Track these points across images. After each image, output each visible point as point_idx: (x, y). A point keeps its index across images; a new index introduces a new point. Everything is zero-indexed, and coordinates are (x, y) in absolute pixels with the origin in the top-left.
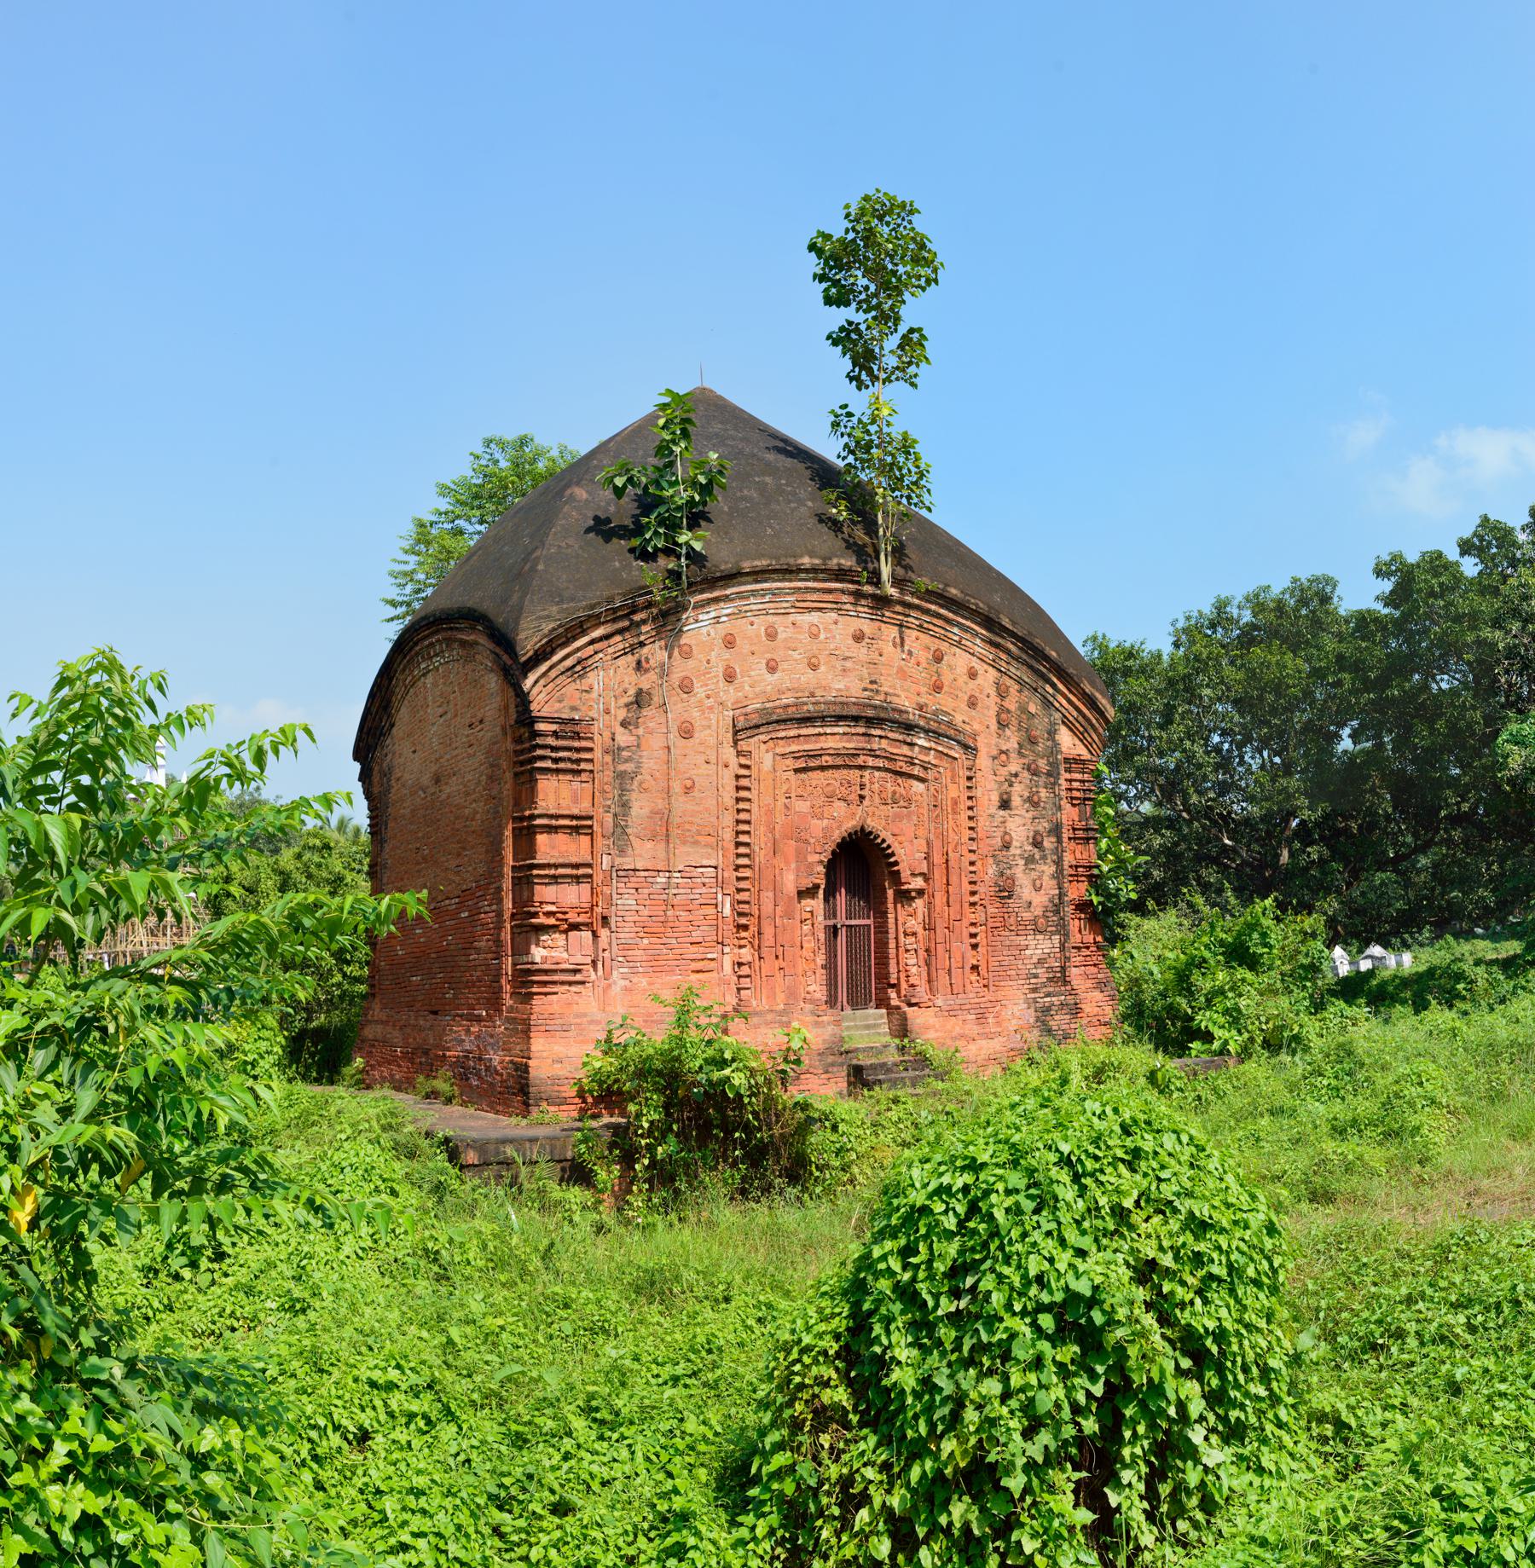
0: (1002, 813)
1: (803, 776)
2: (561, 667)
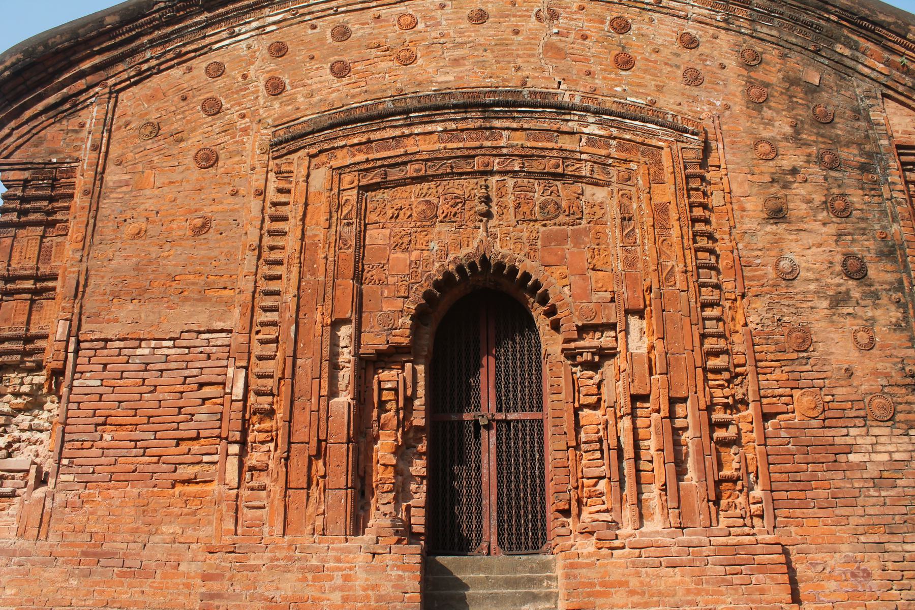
0: (769, 228)
1: (379, 195)
2: (40, 107)
